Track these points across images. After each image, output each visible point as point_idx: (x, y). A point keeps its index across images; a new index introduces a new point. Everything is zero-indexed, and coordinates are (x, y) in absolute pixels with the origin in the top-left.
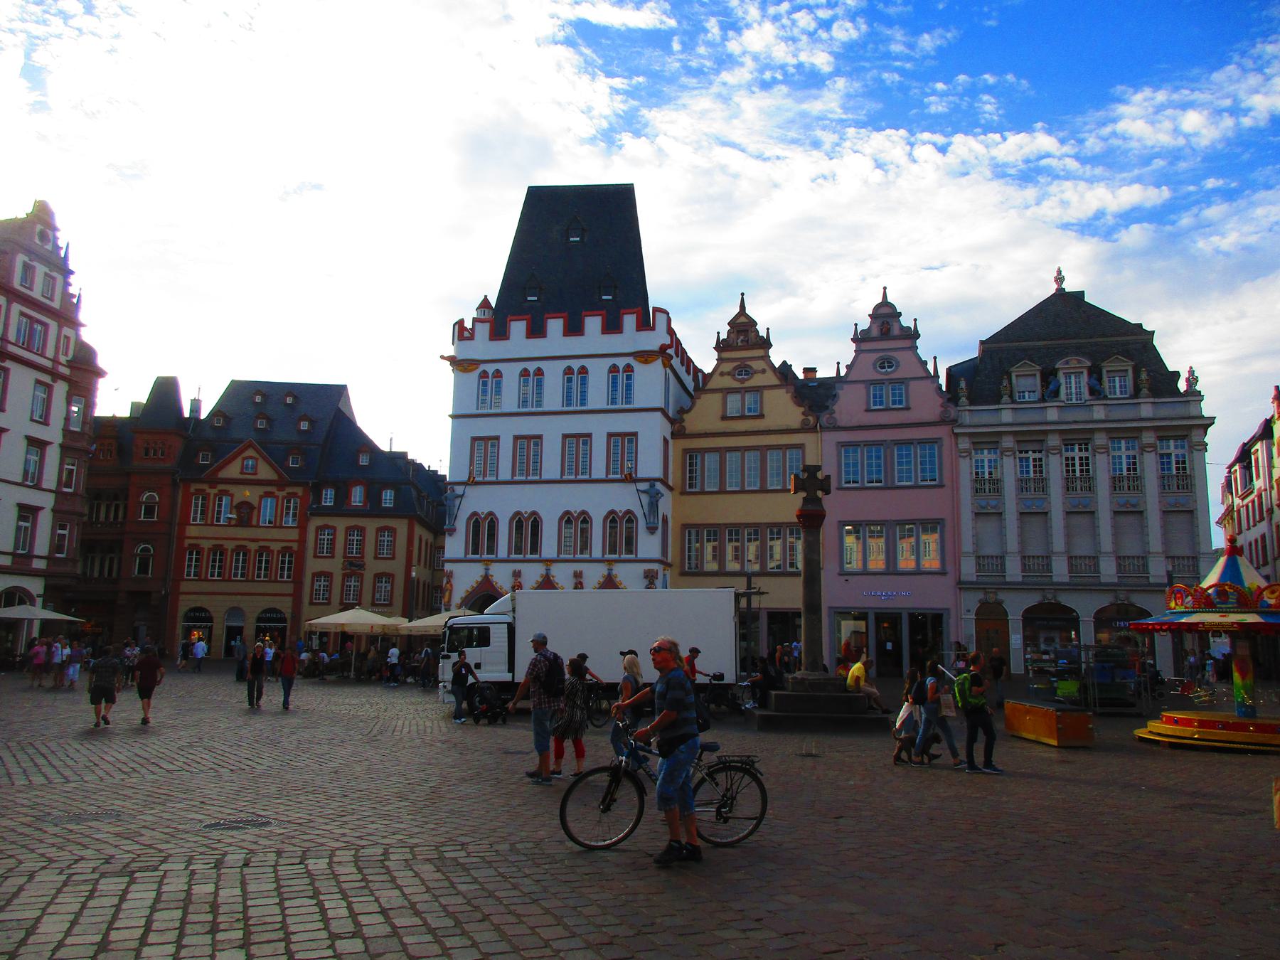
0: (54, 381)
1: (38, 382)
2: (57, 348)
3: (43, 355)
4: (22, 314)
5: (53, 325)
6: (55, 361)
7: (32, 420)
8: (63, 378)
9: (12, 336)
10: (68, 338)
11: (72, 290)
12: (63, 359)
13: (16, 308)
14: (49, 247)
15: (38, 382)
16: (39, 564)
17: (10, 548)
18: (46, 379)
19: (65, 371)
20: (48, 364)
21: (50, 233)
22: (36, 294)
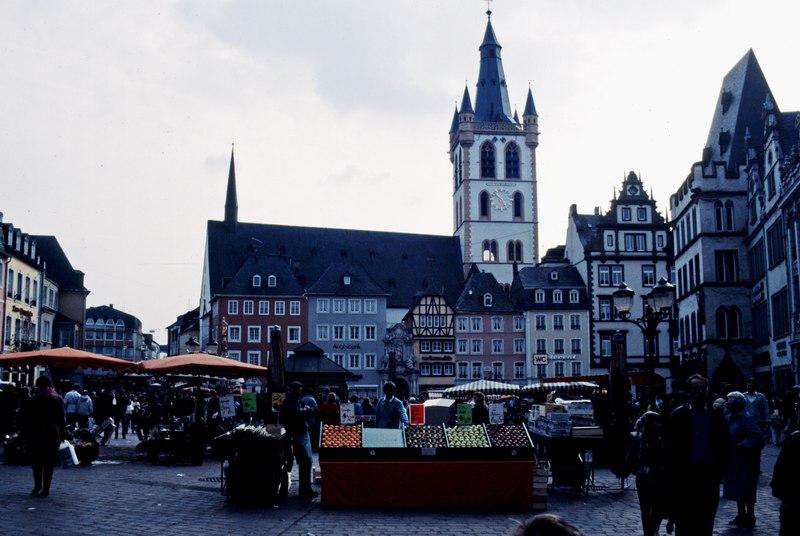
0: (655, 262)
1: (643, 266)
2: (654, 244)
3: (646, 251)
4: (626, 234)
5: (649, 234)
6: (654, 251)
7: (643, 286)
8: (662, 259)
9: (622, 247)
10: (661, 236)
11: (658, 210)
12: (659, 249)
13: (621, 233)
14: (638, 194)
15: (643, 266)
16: (667, 360)
17: (642, 354)
18: (650, 263)
19: (664, 254)
20: (650, 254)
21: (637, 187)
22: (634, 221)
